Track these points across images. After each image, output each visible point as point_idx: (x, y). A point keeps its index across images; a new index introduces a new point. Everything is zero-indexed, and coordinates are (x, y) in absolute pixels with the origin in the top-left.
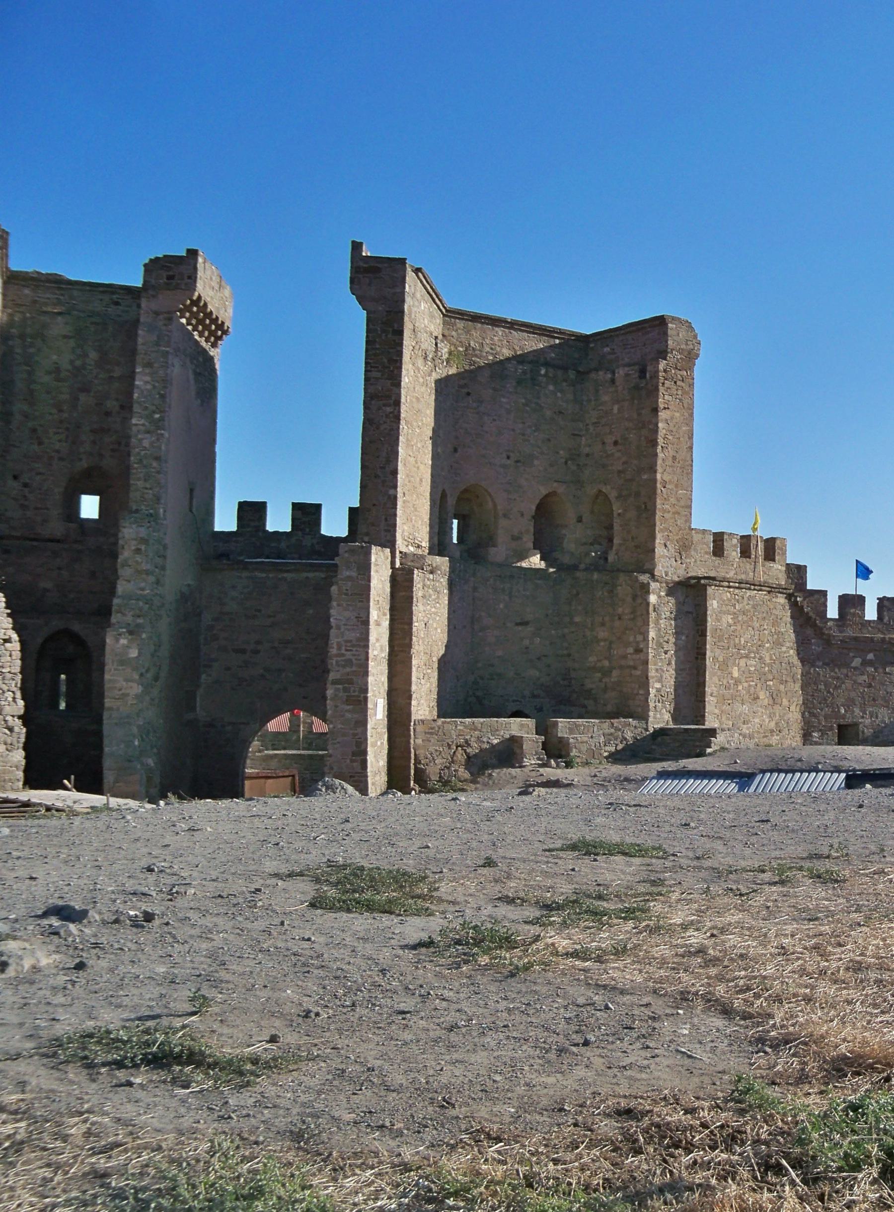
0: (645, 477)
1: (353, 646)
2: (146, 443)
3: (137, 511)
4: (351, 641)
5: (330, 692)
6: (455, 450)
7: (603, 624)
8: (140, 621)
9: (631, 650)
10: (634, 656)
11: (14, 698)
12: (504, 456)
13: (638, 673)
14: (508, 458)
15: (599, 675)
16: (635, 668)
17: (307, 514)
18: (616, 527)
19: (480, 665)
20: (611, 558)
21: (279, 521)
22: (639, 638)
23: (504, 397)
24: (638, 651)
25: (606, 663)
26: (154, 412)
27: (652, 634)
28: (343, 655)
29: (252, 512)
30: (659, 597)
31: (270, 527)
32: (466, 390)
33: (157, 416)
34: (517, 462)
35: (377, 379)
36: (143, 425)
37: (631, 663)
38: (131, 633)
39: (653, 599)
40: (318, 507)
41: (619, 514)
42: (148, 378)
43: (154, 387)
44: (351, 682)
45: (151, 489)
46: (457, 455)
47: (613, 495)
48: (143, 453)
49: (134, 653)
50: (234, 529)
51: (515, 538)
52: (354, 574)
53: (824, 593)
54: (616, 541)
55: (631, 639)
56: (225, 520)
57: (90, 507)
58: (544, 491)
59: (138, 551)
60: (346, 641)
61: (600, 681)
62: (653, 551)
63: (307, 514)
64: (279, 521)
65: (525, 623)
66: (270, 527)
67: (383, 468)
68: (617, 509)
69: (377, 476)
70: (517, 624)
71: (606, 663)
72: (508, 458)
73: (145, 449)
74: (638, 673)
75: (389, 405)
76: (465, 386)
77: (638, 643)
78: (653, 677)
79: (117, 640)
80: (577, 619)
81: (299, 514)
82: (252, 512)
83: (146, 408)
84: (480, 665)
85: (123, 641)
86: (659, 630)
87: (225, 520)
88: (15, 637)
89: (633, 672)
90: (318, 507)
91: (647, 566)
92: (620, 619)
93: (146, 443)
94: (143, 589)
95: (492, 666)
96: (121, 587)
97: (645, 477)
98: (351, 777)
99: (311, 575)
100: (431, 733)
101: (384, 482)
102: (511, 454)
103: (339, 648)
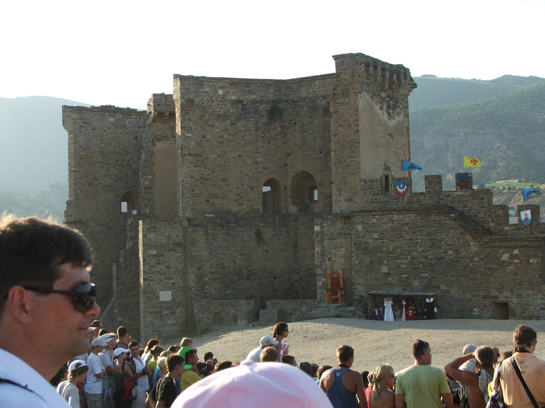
12: (318, 152)
14: (321, 152)
19: (302, 269)
23: (316, 119)
27: (317, 249)
30: (322, 227)
32: (294, 122)
46: (290, 158)
72: (321, 152)
76: (294, 119)
78: (319, 275)
84: (302, 269)
86: (324, 246)
95: (310, 269)
100: (202, 308)
102: (323, 151)
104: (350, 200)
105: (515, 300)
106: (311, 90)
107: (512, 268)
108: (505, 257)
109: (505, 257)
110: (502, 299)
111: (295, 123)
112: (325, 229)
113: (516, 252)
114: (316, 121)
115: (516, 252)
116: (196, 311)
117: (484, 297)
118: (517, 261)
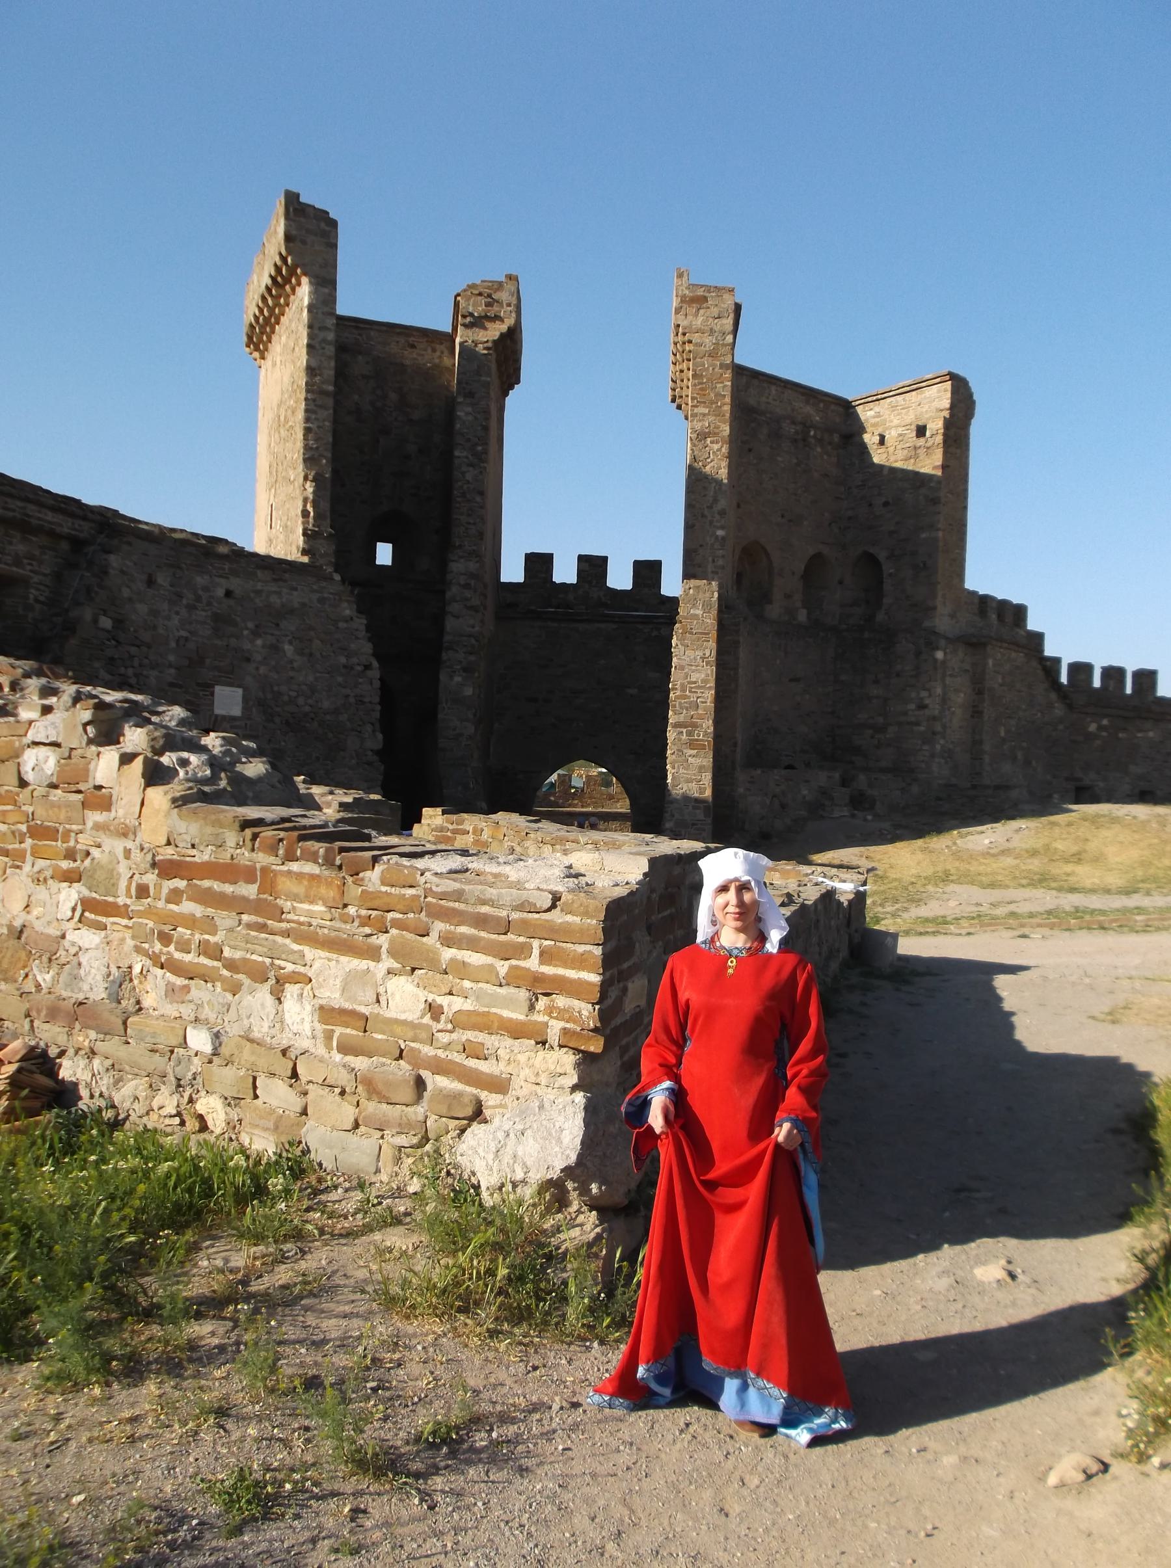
0: (924, 536)
1: (699, 687)
2: (469, 477)
3: (460, 546)
4: (695, 683)
5: (671, 735)
6: (738, 506)
7: (876, 682)
8: (472, 658)
9: (912, 706)
10: (917, 713)
11: (374, 731)
13: (922, 728)
15: (871, 731)
16: (918, 724)
17: (593, 567)
18: (887, 586)
20: (880, 617)
21: (565, 573)
22: (924, 694)
24: (922, 707)
25: (881, 720)
26: (477, 444)
28: (686, 697)
29: (539, 563)
30: (945, 654)
31: (558, 577)
33: (480, 448)
34: (790, 521)
35: (704, 415)
36: (467, 457)
37: (913, 719)
38: (465, 670)
39: (940, 655)
40: (605, 559)
41: (890, 575)
42: (469, 409)
43: (476, 418)
44: (695, 726)
45: (474, 524)
47: (882, 556)
48: (465, 487)
49: (468, 691)
50: (522, 580)
51: (788, 596)
52: (699, 612)
53: (1057, 661)
54: (887, 601)
55: (913, 695)
56: (512, 571)
57: (384, 554)
58: (811, 551)
59: (467, 586)
60: (689, 683)
61: (872, 737)
62: (935, 608)
63: (593, 567)
64: (565, 573)
65: (795, 680)
66: (558, 577)
67: (710, 507)
68: (888, 568)
69: (703, 516)
70: (791, 680)
71: (881, 720)
73: (468, 482)
74: (922, 728)
75: (717, 443)
77: (922, 699)
79: (451, 677)
80: (843, 677)
81: (586, 566)
82: (539, 563)
83: (469, 440)
85: (458, 679)
87: (512, 571)
88: (375, 664)
89: (915, 728)
90: (606, 558)
91: (927, 624)
92: (898, 675)
93: (469, 477)
94: (473, 627)
96: (450, 624)
97: (924, 536)
98: (693, 824)
99: (603, 626)
101: (711, 522)
103: (684, 690)
104: (952, 616)
105: (1101, 784)
106: (764, 399)
107: (1098, 742)
108: (1093, 727)
109: (1093, 727)
110: (1087, 782)
111: (750, 450)
112: (949, 657)
113: (1105, 722)
114: (780, 459)
115: (1105, 722)
116: (741, 790)
117: (1067, 779)
118: (1104, 734)
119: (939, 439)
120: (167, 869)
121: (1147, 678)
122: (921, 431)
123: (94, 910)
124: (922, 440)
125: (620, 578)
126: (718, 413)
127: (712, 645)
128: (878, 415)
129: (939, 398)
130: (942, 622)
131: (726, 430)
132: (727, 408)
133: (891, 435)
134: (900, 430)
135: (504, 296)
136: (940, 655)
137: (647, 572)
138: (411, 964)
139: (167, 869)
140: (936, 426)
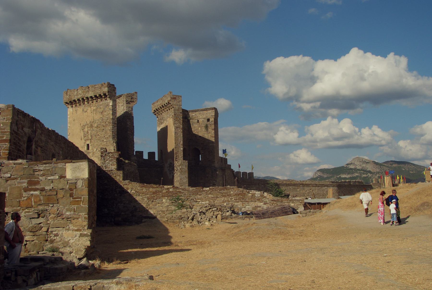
17: (140, 154)
22: (214, 182)
39: (218, 172)
40: (143, 152)
90: (143, 152)
119: (213, 123)
120: (272, 201)
121: (251, 174)
122: (208, 120)
123: (265, 204)
124: (209, 123)
125: (146, 157)
126: (180, 123)
127: (187, 174)
128: (196, 115)
129: (213, 113)
130: (217, 164)
131: (181, 126)
132: (181, 122)
133: (201, 121)
134: (203, 120)
135: (135, 97)
136: (218, 172)
137: (152, 155)
138: (292, 203)
139: (272, 201)
140: (212, 119)
